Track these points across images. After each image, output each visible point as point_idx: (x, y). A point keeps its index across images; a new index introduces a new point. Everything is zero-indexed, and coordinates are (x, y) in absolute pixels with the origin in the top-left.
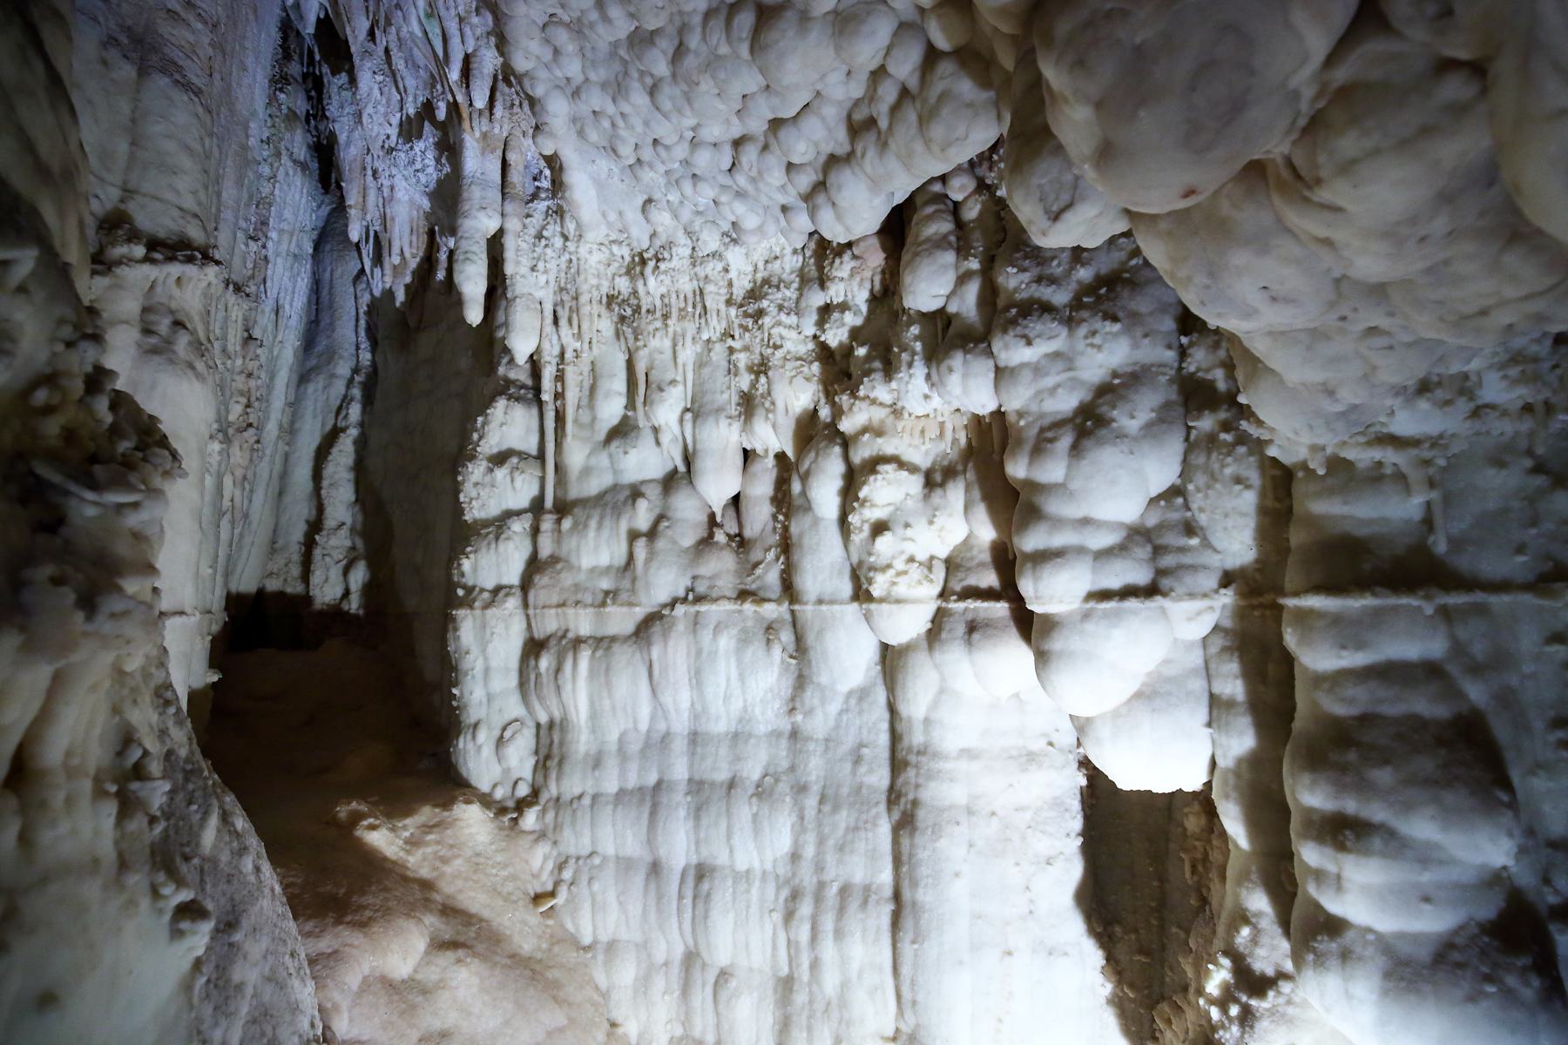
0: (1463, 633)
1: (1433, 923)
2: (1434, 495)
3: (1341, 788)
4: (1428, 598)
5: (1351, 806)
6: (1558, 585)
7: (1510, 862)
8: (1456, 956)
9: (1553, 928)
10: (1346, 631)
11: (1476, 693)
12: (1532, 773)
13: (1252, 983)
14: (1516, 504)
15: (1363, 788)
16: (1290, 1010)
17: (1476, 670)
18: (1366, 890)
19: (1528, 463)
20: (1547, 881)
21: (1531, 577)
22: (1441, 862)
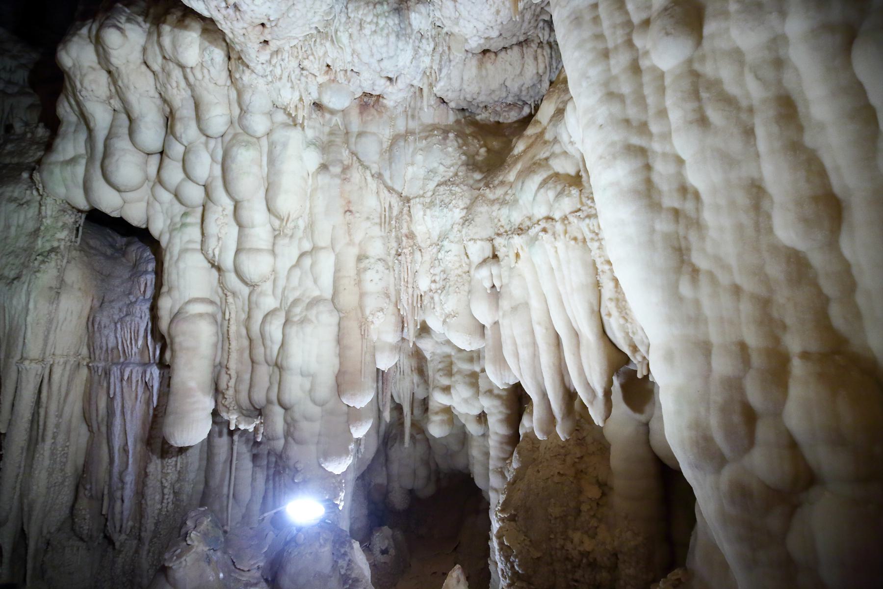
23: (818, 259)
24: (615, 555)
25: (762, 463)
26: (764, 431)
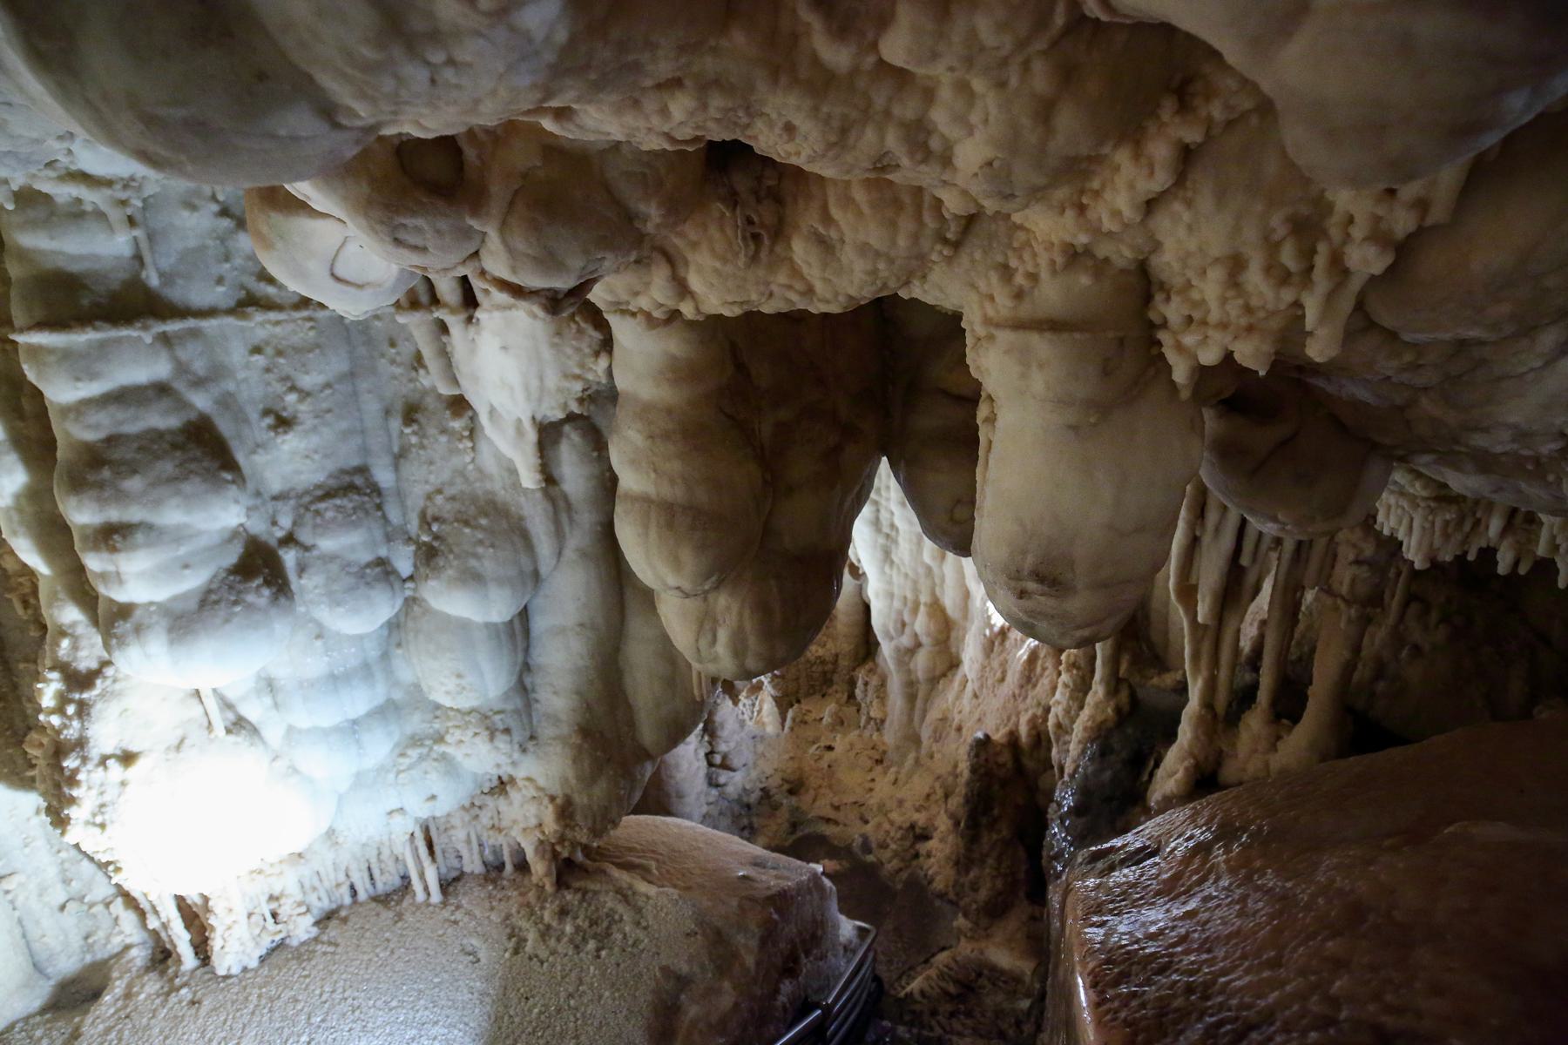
0: (183, 354)
1: (194, 581)
2: (138, 233)
3: (102, 502)
4: (145, 328)
5: (114, 514)
6: (250, 310)
7: (243, 520)
8: (214, 597)
9: (281, 552)
10: (78, 364)
11: (201, 401)
12: (254, 452)
13: (78, 680)
14: (210, 242)
15: (122, 497)
16: (117, 686)
17: (199, 383)
18: (141, 575)
19: (215, 208)
20: (274, 523)
21: (232, 303)
22: (191, 536)
23: (936, 570)
24: (837, 655)
25: (906, 641)
26: (907, 630)
